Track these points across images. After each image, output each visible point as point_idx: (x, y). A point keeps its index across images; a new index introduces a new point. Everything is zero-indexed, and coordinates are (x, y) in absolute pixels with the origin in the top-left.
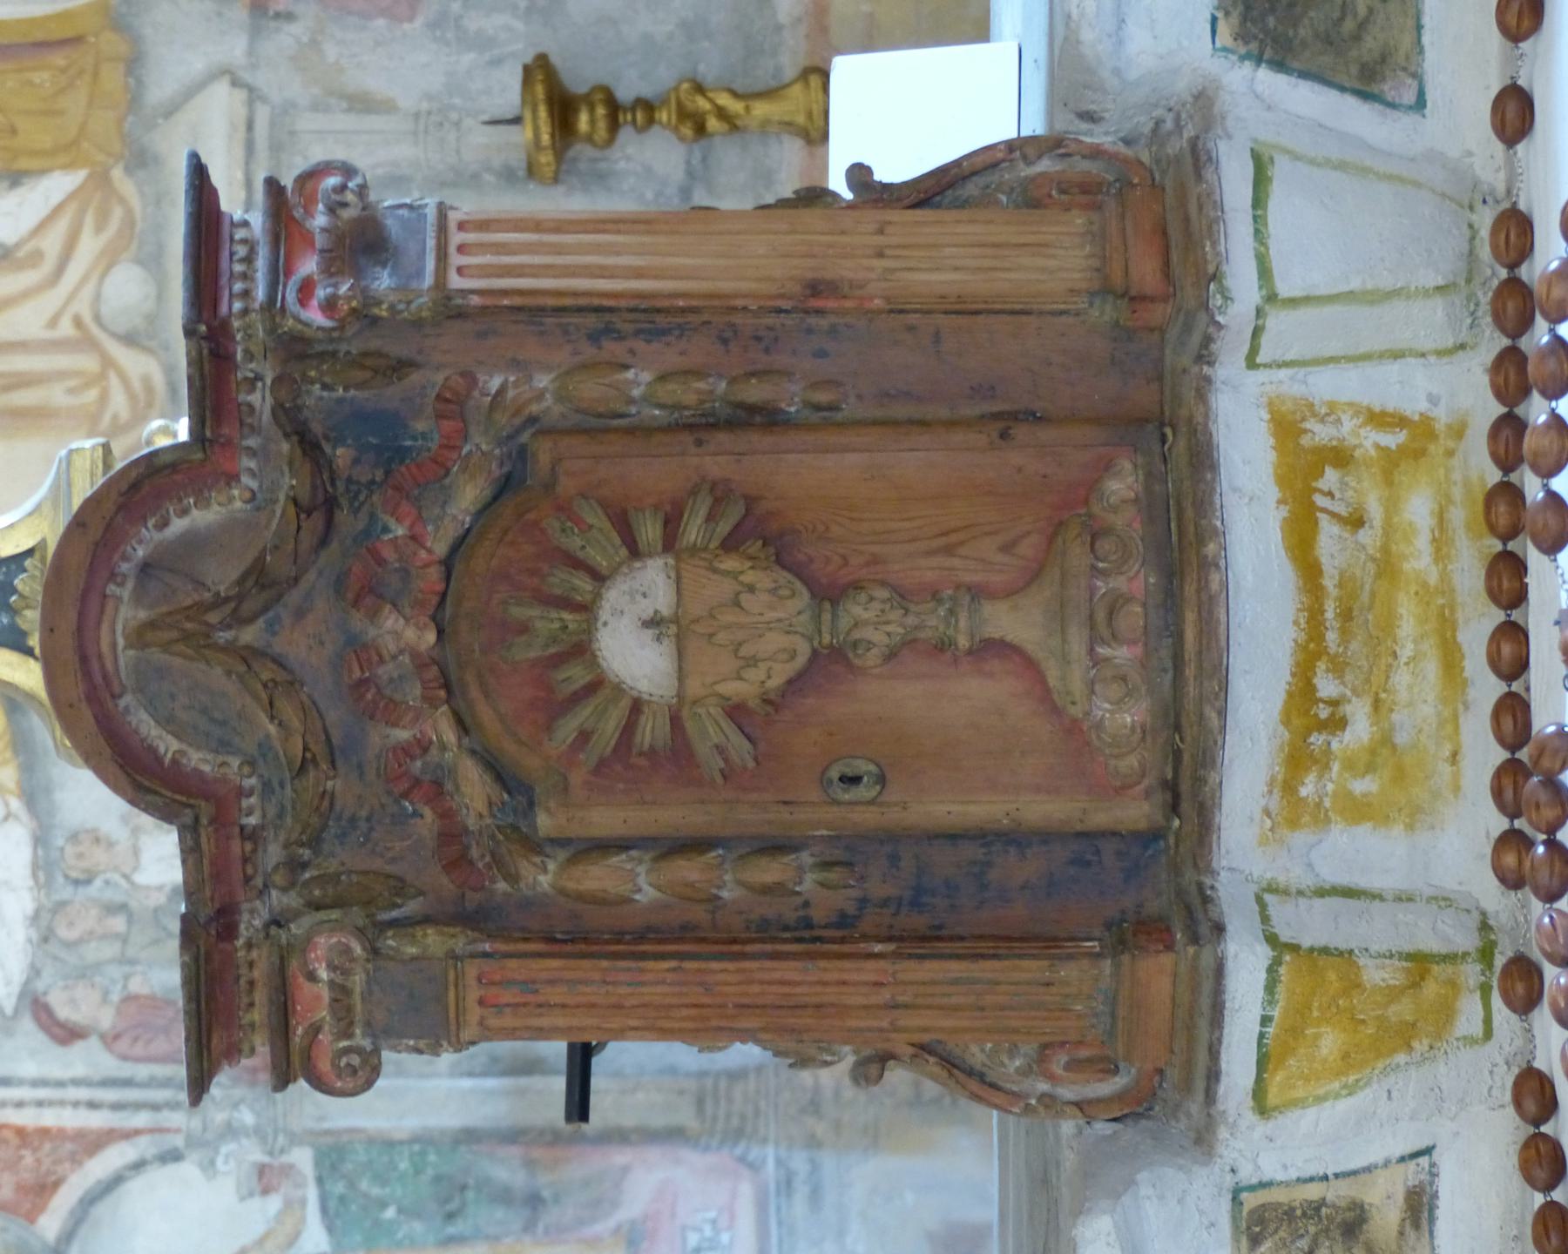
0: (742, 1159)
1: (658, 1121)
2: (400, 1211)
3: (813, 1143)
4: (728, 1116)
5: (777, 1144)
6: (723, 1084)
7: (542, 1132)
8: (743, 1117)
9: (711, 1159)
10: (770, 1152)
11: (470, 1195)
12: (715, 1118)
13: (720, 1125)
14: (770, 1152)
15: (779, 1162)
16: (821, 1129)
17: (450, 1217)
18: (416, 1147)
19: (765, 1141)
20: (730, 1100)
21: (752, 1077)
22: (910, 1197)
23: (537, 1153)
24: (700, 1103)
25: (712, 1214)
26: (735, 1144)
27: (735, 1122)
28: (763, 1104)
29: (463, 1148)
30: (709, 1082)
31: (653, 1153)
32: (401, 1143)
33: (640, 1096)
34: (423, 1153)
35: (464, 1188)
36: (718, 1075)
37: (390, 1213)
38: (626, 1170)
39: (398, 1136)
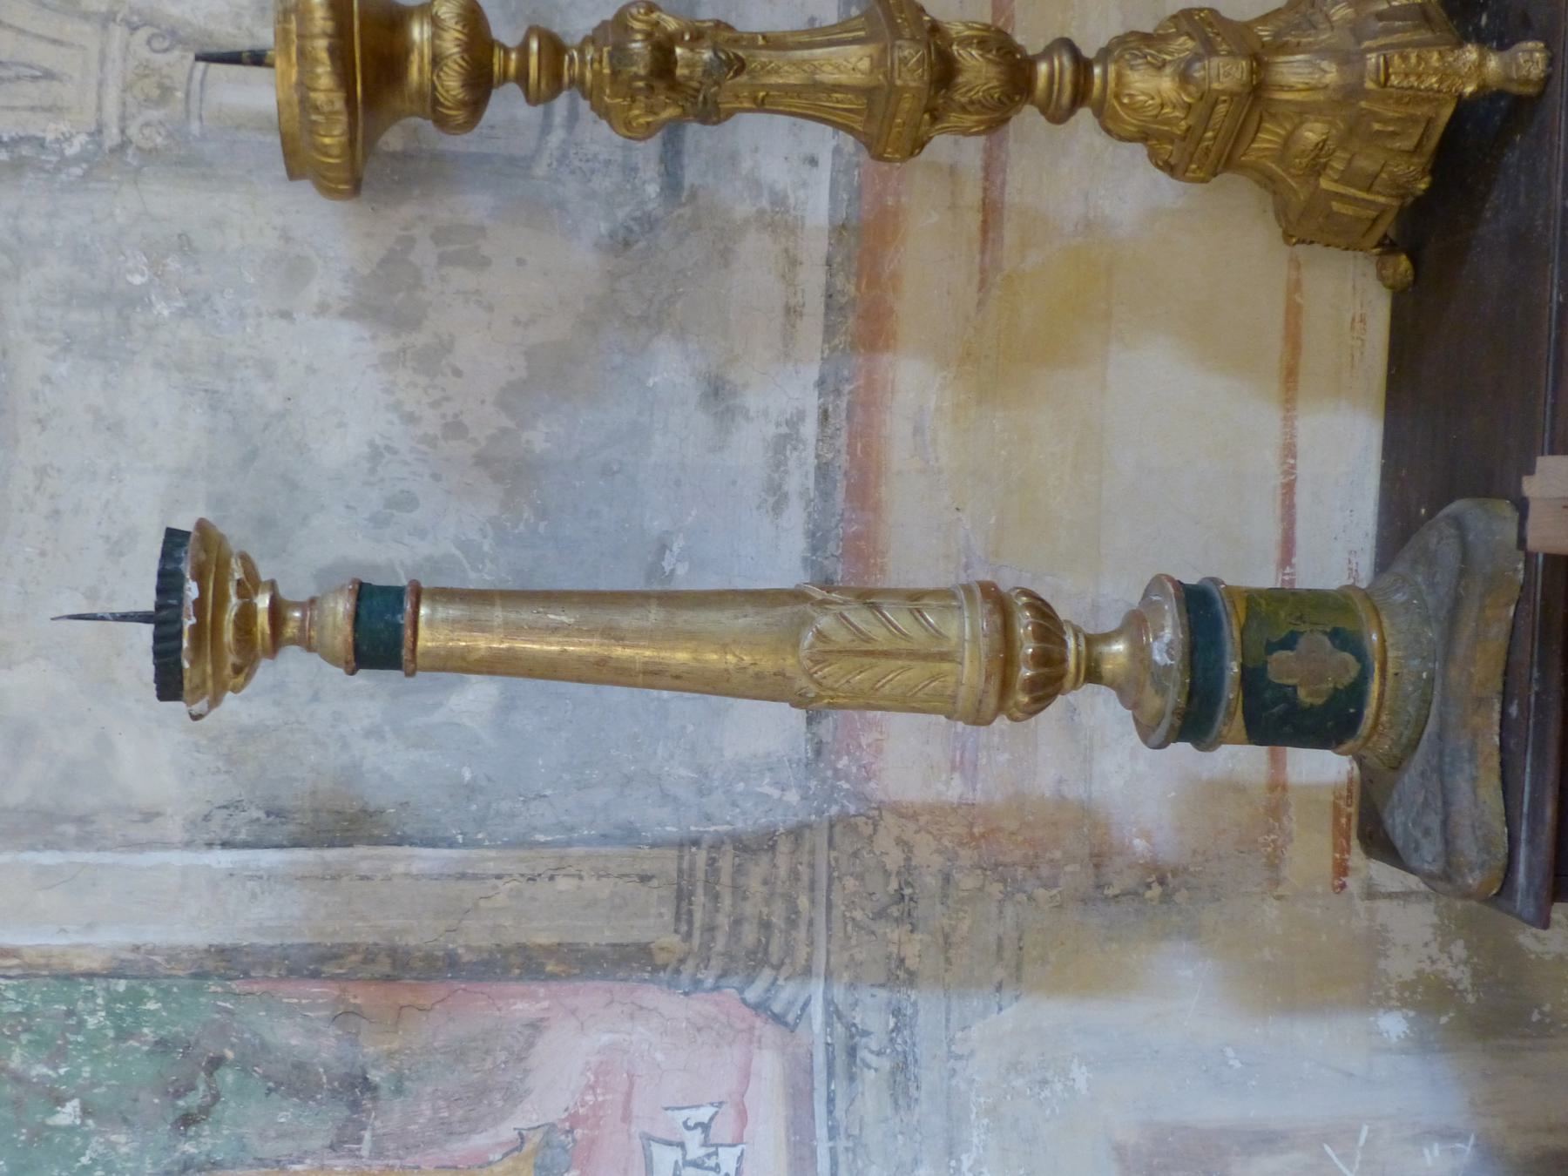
0: (760, 1007)
1: (599, 934)
2: (86, 1112)
3: (900, 974)
4: (737, 922)
5: (829, 976)
6: (726, 864)
7: (370, 956)
8: (766, 926)
9: (701, 1006)
10: (817, 988)
11: (228, 1077)
12: (711, 929)
13: (720, 944)
14: (817, 988)
15: (833, 1013)
16: (913, 948)
17: (187, 1120)
18: (122, 986)
19: (807, 972)
20: (740, 893)
21: (784, 847)
22: (1081, 1076)
23: (358, 997)
24: (683, 896)
25: (704, 1114)
26: (750, 980)
27: (750, 934)
28: (803, 902)
29: (213, 986)
30: (702, 857)
31: (590, 995)
32: (90, 975)
33: (563, 884)
34: (137, 997)
35: (216, 1063)
36: (717, 845)
37: (68, 1114)
38: (536, 1027)
39: (82, 964)
